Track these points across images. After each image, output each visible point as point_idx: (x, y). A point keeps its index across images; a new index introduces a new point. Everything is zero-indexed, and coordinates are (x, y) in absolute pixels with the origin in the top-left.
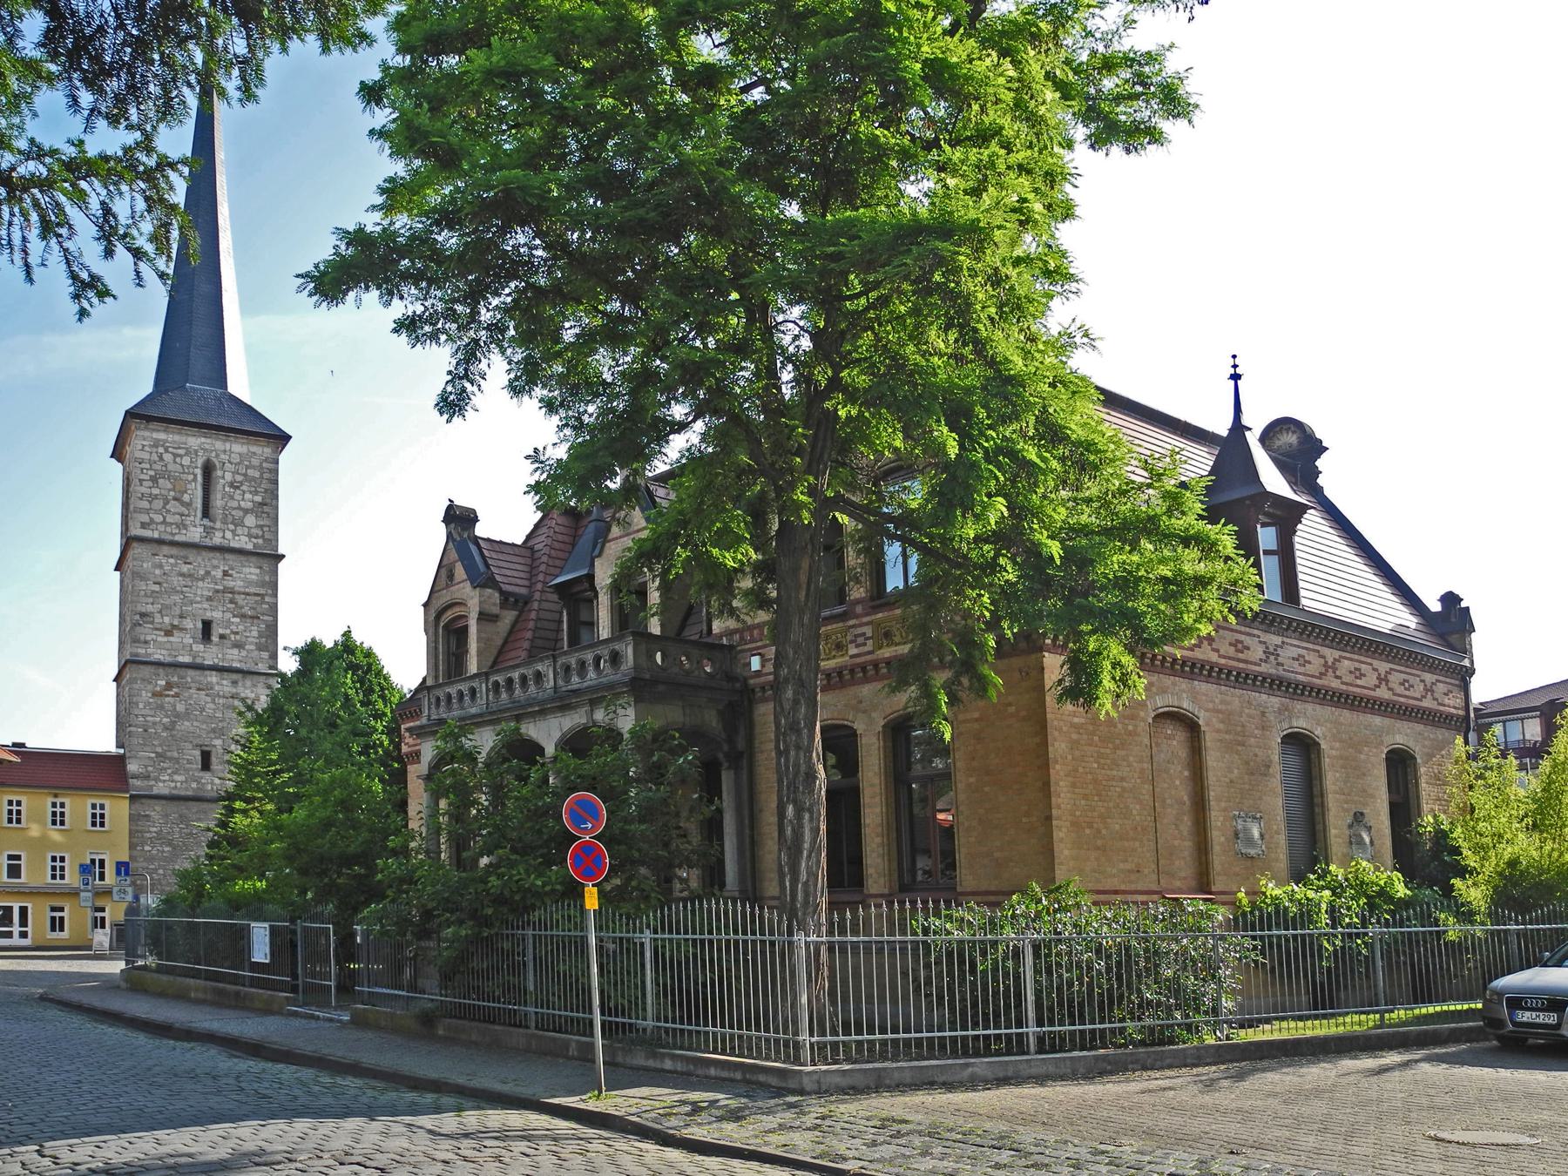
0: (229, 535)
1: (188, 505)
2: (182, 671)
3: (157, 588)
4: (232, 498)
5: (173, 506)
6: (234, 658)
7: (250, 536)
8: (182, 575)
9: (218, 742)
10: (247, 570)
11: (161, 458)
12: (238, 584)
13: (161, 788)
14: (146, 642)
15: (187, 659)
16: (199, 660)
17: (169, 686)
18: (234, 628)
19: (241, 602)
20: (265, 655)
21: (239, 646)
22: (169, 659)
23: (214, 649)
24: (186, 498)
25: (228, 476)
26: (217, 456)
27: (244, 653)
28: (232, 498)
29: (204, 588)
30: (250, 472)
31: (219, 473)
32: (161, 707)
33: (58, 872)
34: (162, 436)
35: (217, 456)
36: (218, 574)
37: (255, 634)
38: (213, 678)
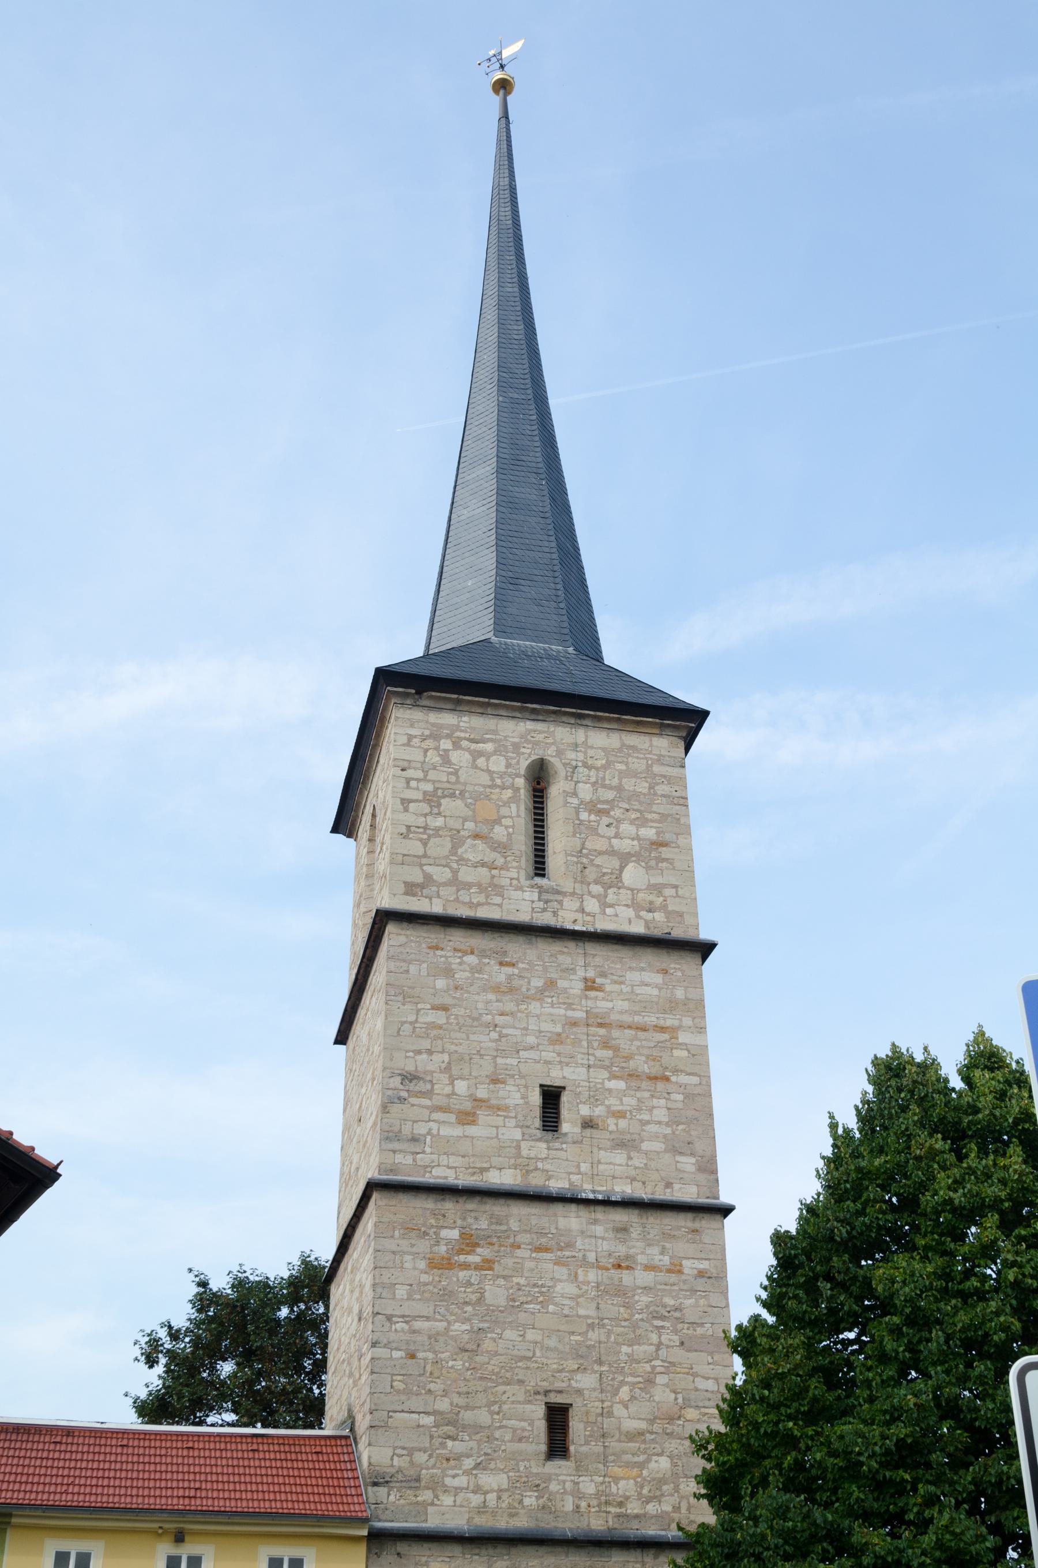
0: (592, 905)
3: (440, 1018)
4: (594, 831)
5: (475, 851)
7: (635, 905)
8: (497, 989)
9: (586, 1381)
11: (446, 760)
12: (612, 1004)
13: (447, 1514)
14: (414, 1139)
16: (536, 1182)
17: (469, 1242)
18: (612, 1101)
19: (624, 1045)
20: (688, 1163)
21: (625, 1144)
22: (464, 1180)
24: (499, 833)
25: (585, 792)
26: (560, 753)
27: (638, 1161)
28: (594, 831)
29: (545, 1016)
30: (629, 784)
32: (446, 1295)
34: (448, 719)
35: (560, 753)
36: (576, 987)
37: (660, 1114)
38: (571, 1219)
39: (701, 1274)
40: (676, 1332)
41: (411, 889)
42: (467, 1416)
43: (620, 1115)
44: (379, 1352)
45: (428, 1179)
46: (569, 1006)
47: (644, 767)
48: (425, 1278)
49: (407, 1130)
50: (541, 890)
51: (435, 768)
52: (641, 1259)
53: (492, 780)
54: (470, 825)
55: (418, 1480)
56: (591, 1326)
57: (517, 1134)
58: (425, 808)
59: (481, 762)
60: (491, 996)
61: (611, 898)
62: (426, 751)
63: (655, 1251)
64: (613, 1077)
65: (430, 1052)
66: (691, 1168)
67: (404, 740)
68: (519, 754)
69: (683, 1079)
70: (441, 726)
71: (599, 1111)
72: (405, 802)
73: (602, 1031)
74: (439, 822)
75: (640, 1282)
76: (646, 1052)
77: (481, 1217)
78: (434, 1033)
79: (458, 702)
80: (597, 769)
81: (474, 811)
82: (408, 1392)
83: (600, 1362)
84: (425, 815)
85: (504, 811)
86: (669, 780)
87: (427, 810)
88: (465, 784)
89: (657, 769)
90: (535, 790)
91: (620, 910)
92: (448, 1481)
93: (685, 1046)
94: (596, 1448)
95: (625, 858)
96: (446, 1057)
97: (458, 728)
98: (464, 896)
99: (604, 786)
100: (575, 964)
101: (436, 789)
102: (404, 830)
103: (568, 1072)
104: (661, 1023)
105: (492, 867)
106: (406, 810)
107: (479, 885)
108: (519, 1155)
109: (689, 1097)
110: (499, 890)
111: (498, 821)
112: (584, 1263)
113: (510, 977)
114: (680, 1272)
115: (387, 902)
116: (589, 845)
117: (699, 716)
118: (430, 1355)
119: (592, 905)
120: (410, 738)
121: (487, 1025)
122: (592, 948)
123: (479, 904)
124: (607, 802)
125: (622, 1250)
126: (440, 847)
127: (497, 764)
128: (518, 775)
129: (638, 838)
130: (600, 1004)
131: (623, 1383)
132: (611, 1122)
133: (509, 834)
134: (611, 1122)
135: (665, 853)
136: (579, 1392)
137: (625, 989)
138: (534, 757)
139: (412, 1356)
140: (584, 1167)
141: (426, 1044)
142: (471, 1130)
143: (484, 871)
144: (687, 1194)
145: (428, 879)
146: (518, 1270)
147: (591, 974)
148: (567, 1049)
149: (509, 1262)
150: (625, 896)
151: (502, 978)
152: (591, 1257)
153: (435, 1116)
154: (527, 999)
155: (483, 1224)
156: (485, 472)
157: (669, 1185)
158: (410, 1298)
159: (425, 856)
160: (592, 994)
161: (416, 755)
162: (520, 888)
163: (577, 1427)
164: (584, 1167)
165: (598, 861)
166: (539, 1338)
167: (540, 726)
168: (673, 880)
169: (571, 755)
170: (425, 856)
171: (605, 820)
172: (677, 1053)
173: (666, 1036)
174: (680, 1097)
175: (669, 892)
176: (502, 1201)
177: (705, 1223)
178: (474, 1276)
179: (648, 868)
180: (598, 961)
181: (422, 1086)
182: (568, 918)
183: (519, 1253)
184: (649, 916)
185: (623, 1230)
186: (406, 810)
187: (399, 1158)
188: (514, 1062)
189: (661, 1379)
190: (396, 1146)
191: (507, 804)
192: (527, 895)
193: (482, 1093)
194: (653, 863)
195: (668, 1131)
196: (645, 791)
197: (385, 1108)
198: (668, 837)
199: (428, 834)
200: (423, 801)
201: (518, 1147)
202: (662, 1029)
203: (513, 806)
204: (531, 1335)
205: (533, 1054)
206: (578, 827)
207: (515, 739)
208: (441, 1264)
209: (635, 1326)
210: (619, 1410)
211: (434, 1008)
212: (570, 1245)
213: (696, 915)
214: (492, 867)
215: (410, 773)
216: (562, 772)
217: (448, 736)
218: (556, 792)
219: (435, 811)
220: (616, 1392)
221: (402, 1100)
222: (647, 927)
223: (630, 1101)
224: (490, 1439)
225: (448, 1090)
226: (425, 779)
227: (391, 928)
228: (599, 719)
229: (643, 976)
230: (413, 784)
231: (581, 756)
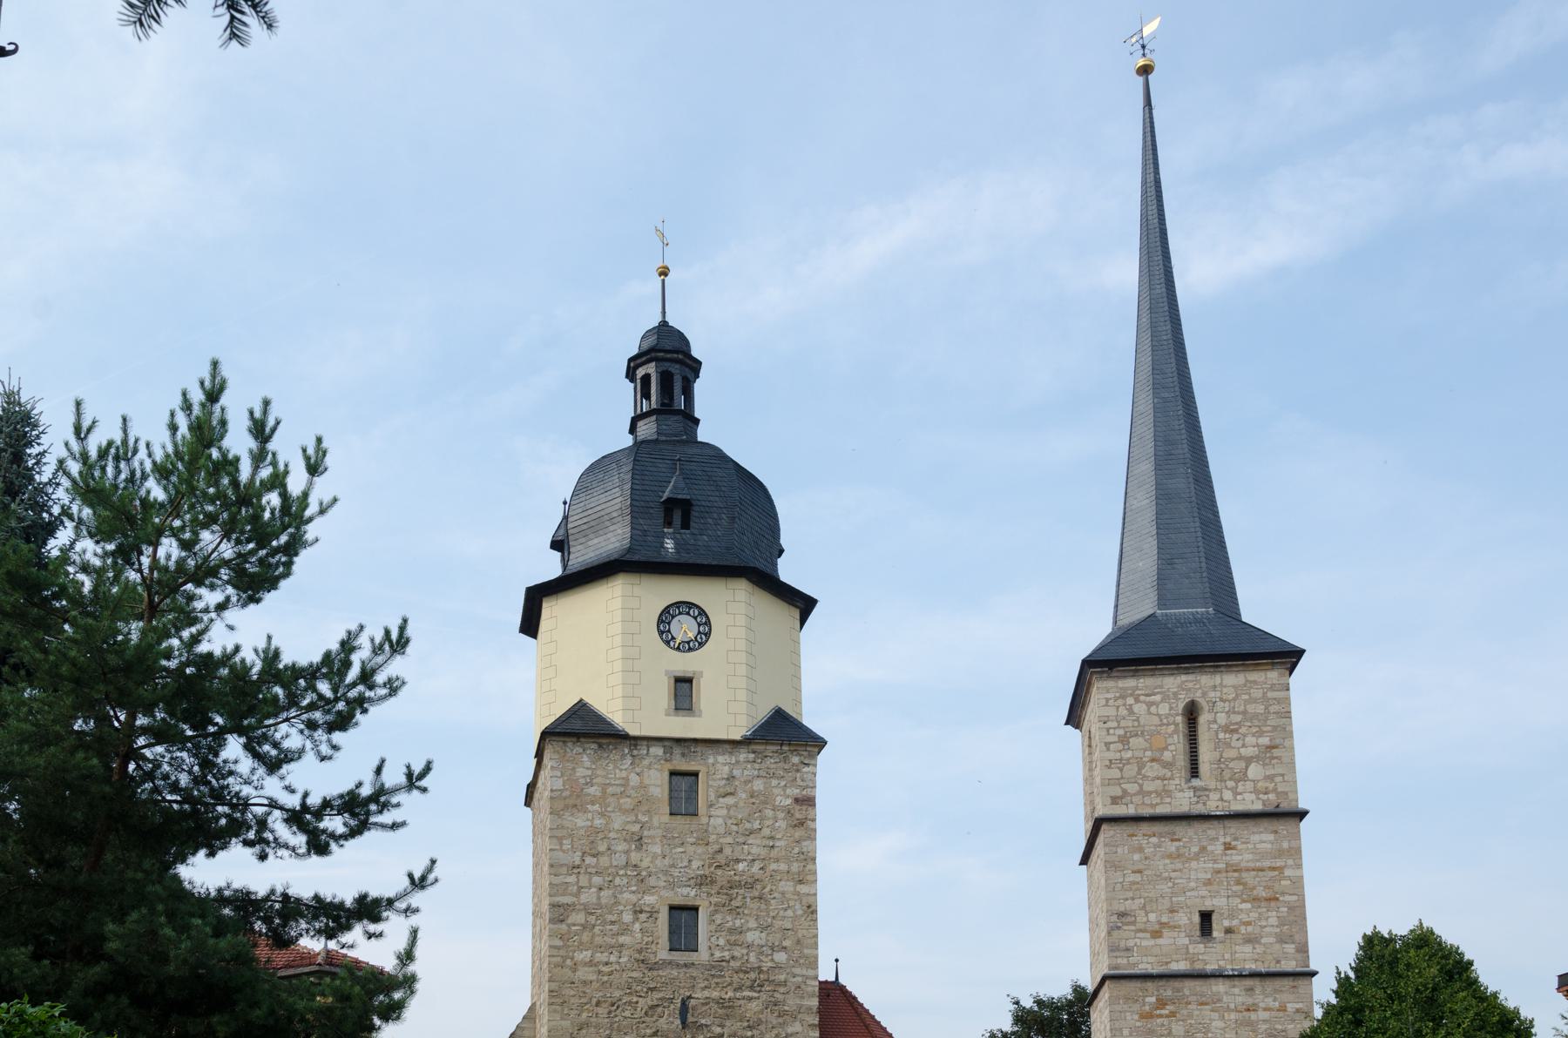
0: (1228, 795)
1: (1168, 765)
2: (1177, 984)
3: (1138, 877)
4: (1229, 745)
5: (1152, 770)
6: (1247, 958)
7: (1256, 791)
8: (1170, 856)
10: (1256, 838)
11: (1131, 711)
12: (1242, 857)
14: (1127, 950)
15: (1181, 966)
16: (1198, 966)
17: (1161, 1003)
18: (1244, 917)
20: (1290, 948)
21: (1250, 940)
23: (1219, 947)
24: (1167, 756)
25: (1222, 719)
26: (1204, 694)
27: (1259, 949)
28: (1229, 745)
29: (1201, 869)
34: (1130, 683)
35: (1204, 694)
36: (1219, 848)
37: (1273, 921)
38: (1220, 987)
39: (1298, 1011)
41: (1115, 800)
43: (1249, 923)
46: (1215, 861)
49: (1122, 944)
57: (1186, 941)
58: (1120, 746)
59: (1153, 709)
64: (1244, 901)
69: (1287, 898)
70: (1125, 689)
71: (1235, 922)
72: (1107, 744)
74: (1129, 754)
77: (1168, 990)
85: (1170, 741)
86: (1279, 701)
89: (1270, 694)
91: (1246, 796)
93: (1289, 878)
95: (1248, 761)
97: (1137, 688)
100: (1218, 835)
105: (1163, 779)
110: (1168, 793)
111: (1166, 748)
112: (1228, 1009)
113: (1178, 849)
115: (1101, 811)
117: (1298, 654)
119: (1228, 795)
120: (1107, 700)
122: (1228, 823)
125: (1250, 1001)
126: (1130, 771)
127: (1164, 709)
135: (1276, 752)
140: (1227, 956)
144: (1289, 966)
145: (1125, 792)
146: (1190, 1016)
147: (1228, 839)
148: (1215, 887)
150: (1249, 785)
152: (1232, 1006)
154: (1189, 860)
155: (1169, 993)
156: (1146, 468)
161: (1111, 712)
162: (1182, 791)
164: (1227, 956)
165: (1231, 765)
167: (1191, 677)
168: (1280, 771)
169: (1212, 694)
171: (1236, 736)
175: (1278, 779)
177: (1301, 982)
182: (1213, 805)
185: (1251, 990)
191: (1171, 735)
193: (1164, 919)
197: (1109, 933)
198: (1278, 741)
199: (1123, 763)
202: (1274, 869)
206: (1218, 744)
207: (1176, 687)
208: (1147, 1016)
212: (1219, 1000)
213: (1296, 792)
214: (1163, 779)
215: (1109, 724)
216: (1206, 708)
218: (1203, 719)
223: (1254, 915)
227: (1104, 827)
229: (1262, 838)
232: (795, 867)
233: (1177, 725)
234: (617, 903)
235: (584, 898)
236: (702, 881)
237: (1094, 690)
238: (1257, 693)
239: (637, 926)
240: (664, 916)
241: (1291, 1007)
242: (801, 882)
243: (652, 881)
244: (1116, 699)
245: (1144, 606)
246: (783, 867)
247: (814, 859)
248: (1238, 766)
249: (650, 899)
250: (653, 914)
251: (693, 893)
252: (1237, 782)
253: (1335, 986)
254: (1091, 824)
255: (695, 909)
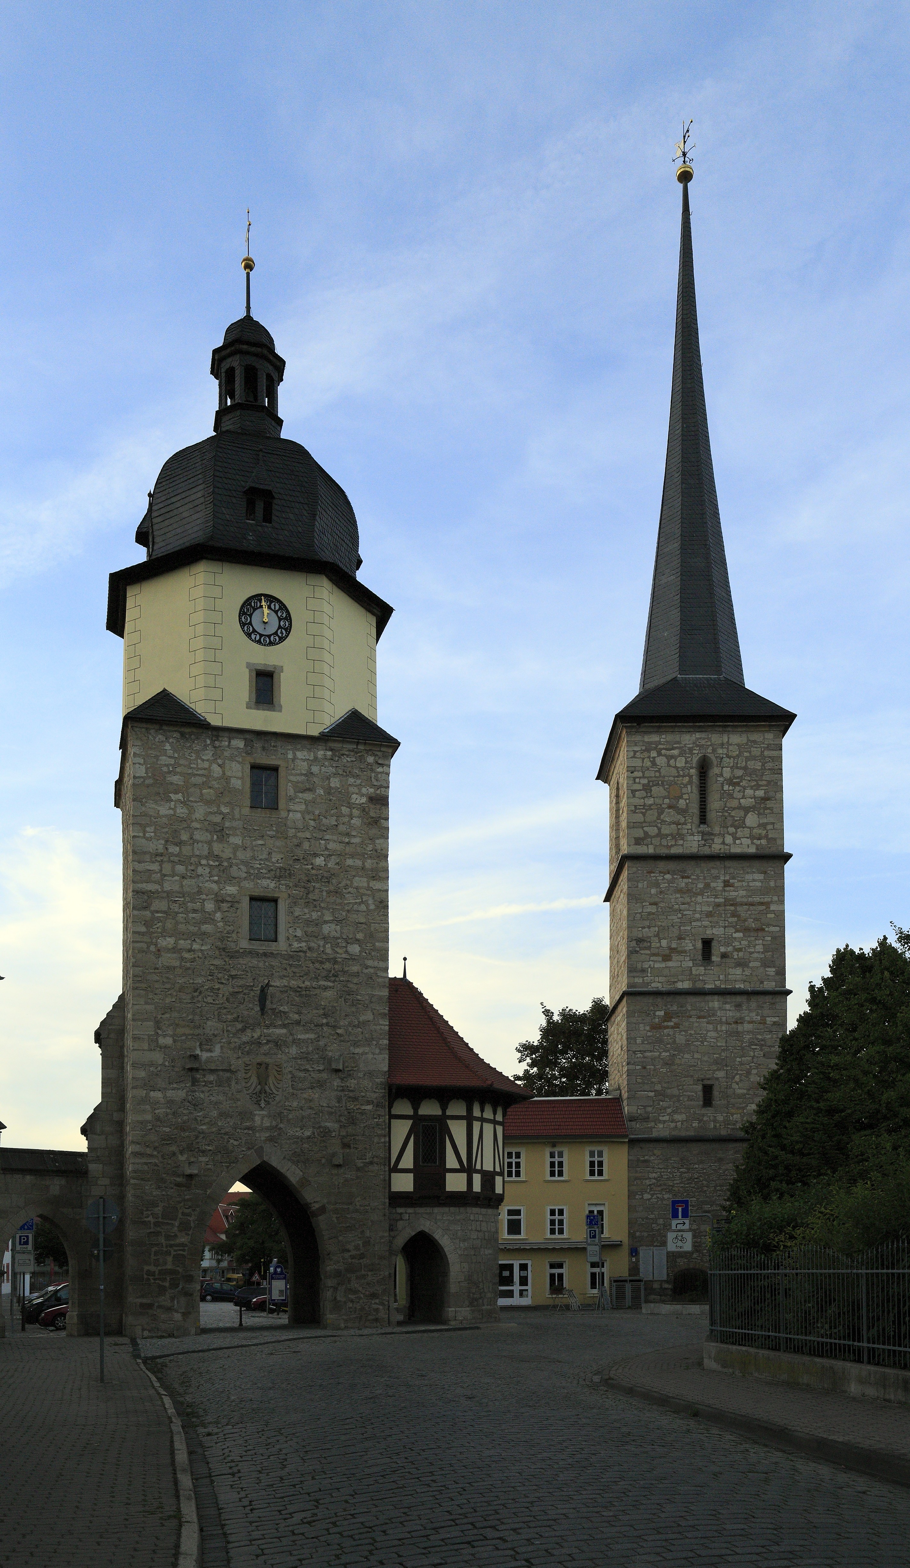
0: (729, 839)
1: (683, 812)
2: (681, 999)
3: (653, 909)
4: (731, 796)
5: (669, 816)
6: (737, 978)
7: (752, 837)
8: (680, 891)
9: (720, 1074)
10: (749, 877)
11: (654, 763)
12: (739, 894)
13: (660, 1130)
14: (643, 971)
15: (685, 985)
16: (699, 985)
17: (668, 1017)
20: (771, 971)
22: (667, 988)
24: (682, 803)
25: (727, 773)
26: (714, 750)
27: (748, 972)
28: (731, 796)
29: (704, 904)
31: (716, 770)
32: (660, 1041)
33: (556, 1226)
34: (655, 738)
35: (714, 750)
37: (760, 948)
38: (715, 1003)
39: (775, 1023)
40: (761, 1050)
41: (638, 841)
42: (669, 1091)
43: (740, 950)
44: (631, 1067)
45: (649, 989)
47: (759, 754)
48: (649, 1034)
49: (639, 966)
50: (703, 834)
51: (648, 769)
52: (747, 1018)
53: (678, 772)
54: (667, 801)
55: (648, 1118)
56: (723, 1050)
57: (690, 964)
58: (643, 793)
59: (672, 762)
60: (678, 895)
61: (739, 834)
62: (643, 759)
63: (754, 1014)
64: (737, 931)
65: (649, 927)
66: (773, 973)
67: (632, 754)
68: (692, 754)
69: (772, 929)
70: (651, 743)
71: (730, 949)
73: (732, 908)
74: (650, 801)
75: (745, 1029)
76: (753, 917)
78: (651, 917)
79: (659, 727)
80: (734, 758)
81: (669, 792)
82: (643, 1083)
83: (726, 1066)
84: (644, 798)
85: (684, 790)
87: (645, 794)
88: (664, 777)
89: (766, 753)
90: (701, 773)
91: (744, 840)
92: (661, 1118)
94: (724, 1102)
95: (747, 810)
96: (657, 929)
97: (660, 743)
98: (664, 842)
99: (737, 768)
101: (649, 782)
102: (633, 808)
103: (715, 931)
104: (762, 900)
105: (678, 824)
106: (634, 796)
107: (671, 835)
108: (691, 974)
109: (774, 938)
110: (682, 837)
111: (681, 797)
112: (721, 1023)
113: (687, 884)
114: (765, 1023)
116: (728, 805)
118: (652, 1067)
120: (635, 752)
121: (676, 911)
122: (728, 863)
123: (672, 846)
124: (738, 778)
125: (738, 1014)
126: (652, 815)
127: (681, 762)
128: (692, 768)
129: (755, 797)
130: (731, 894)
131: (737, 1074)
132: (735, 954)
133: (687, 804)
134: (735, 954)
135: (769, 804)
136: (717, 1079)
137: (745, 884)
138: (700, 755)
139: (645, 1068)
141: (647, 923)
142: (670, 964)
143: (673, 826)
145: (646, 833)
147: (727, 878)
148: (715, 919)
149: (687, 1024)
150: (747, 832)
151: (683, 885)
152: (724, 1019)
153: (652, 958)
154: (696, 894)
155: (675, 1008)
157: (762, 982)
158: (643, 1043)
159: (645, 822)
160: (727, 889)
161: (638, 763)
162: (693, 835)
163: (716, 1093)
164: (722, 977)
166: (699, 1057)
167: (703, 735)
168: (772, 820)
169: (720, 751)
170: (645, 822)
171: (738, 788)
172: (769, 916)
173: (764, 907)
174: (769, 938)
176: (683, 996)
177: (778, 999)
178: (671, 1031)
179: (759, 814)
180: (732, 870)
181: (646, 944)
183: (691, 1020)
184: (758, 842)
186: (634, 796)
187: (636, 980)
188: (689, 928)
189: (754, 1071)
190: (635, 974)
191: (686, 786)
192: (696, 838)
193: (674, 945)
194: (762, 811)
195: (762, 956)
196: (759, 768)
200: (643, 790)
201: (691, 970)
202: (762, 904)
203: (689, 787)
204: (696, 1056)
205: (699, 924)
209: (743, 1049)
210: (734, 1086)
211: (650, 904)
212: (714, 1015)
214: (678, 824)
216: (715, 763)
217: (655, 749)
219: (649, 794)
220: (734, 1077)
221: (637, 952)
222: (757, 849)
223: (744, 943)
224: (679, 1101)
225: (658, 945)
226: (644, 777)
228: (736, 726)
230: (637, 780)
231: (725, 751)
232: (369, 864)
233: (691, 777)
234: (200, 892)
235: (167, 887)
236: (282, 874)
237: (624, 744)
238: (756, 751)
239: (218, 916)
240: (245, 903)
241: (769, 1020)
242: (373, 878)
243: (234, 871)
244: (642, 751)
245: (670, 671)
246: (359, 863)
247: (386, 856)
248: (738, 814)
249: (231, 889)
250: (234, 903)
251: (272, 885)
252: (737, 828)
253: (808, 996)
254: (616, 864)
255: (275, 901)
